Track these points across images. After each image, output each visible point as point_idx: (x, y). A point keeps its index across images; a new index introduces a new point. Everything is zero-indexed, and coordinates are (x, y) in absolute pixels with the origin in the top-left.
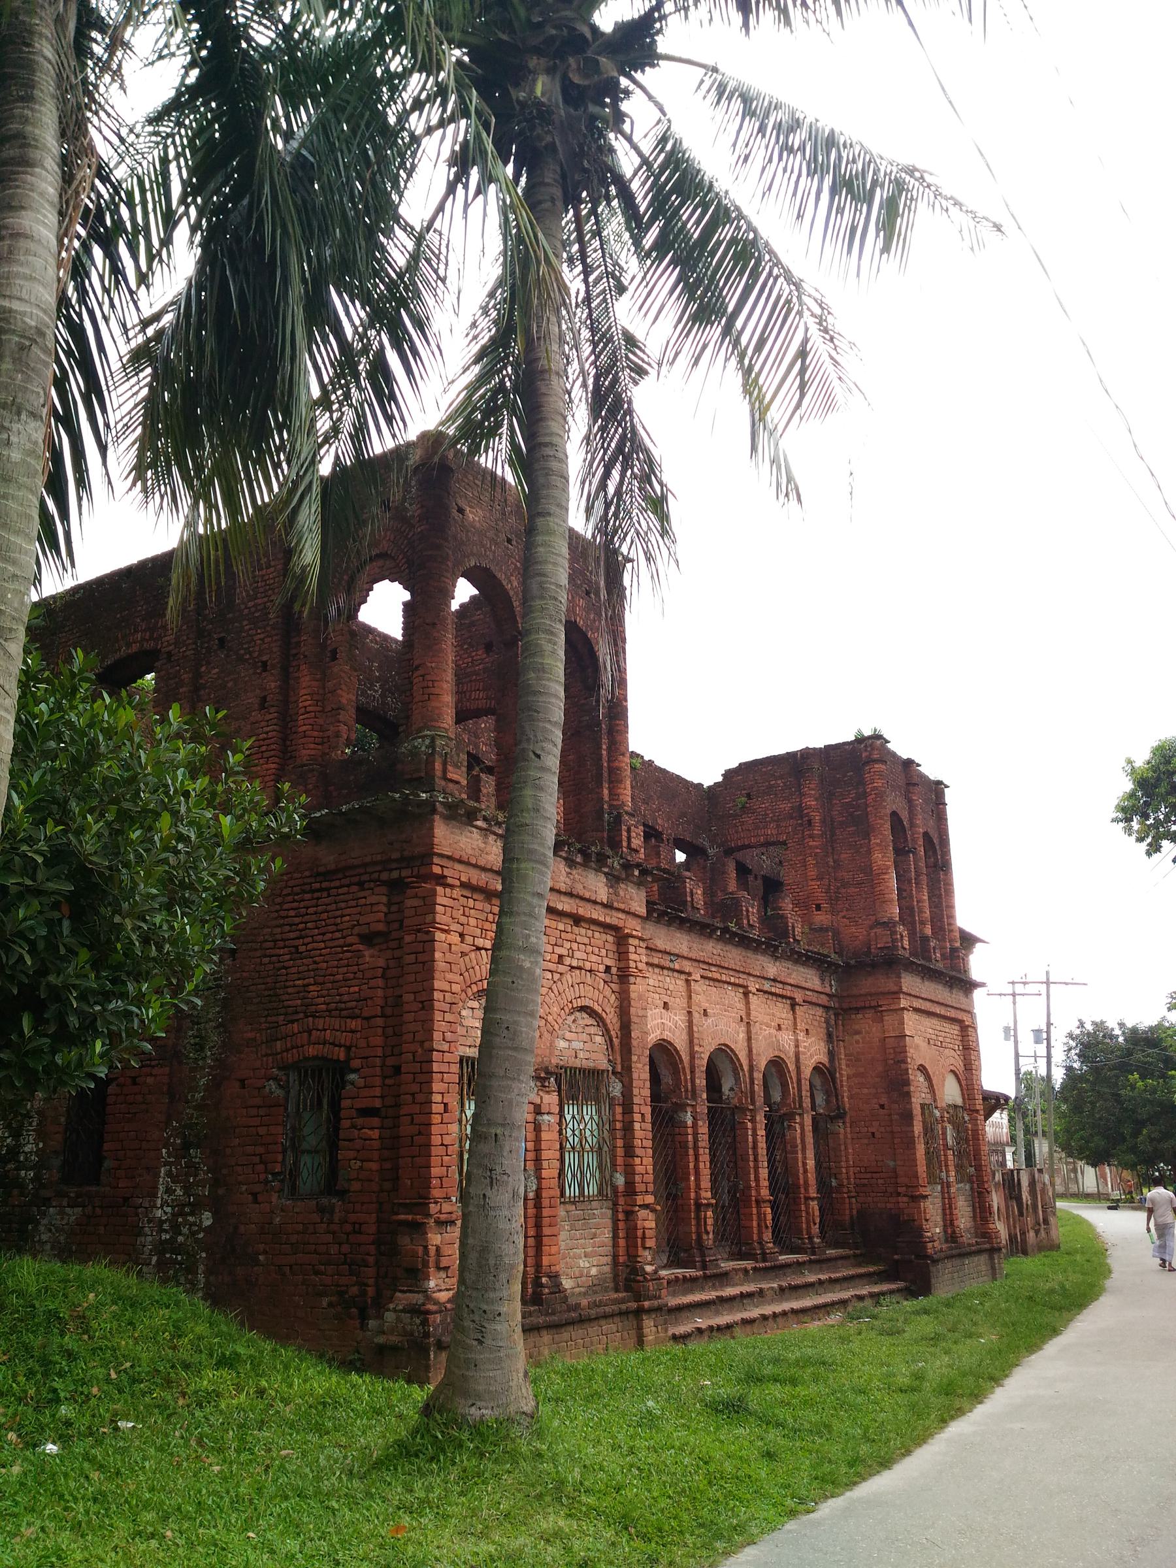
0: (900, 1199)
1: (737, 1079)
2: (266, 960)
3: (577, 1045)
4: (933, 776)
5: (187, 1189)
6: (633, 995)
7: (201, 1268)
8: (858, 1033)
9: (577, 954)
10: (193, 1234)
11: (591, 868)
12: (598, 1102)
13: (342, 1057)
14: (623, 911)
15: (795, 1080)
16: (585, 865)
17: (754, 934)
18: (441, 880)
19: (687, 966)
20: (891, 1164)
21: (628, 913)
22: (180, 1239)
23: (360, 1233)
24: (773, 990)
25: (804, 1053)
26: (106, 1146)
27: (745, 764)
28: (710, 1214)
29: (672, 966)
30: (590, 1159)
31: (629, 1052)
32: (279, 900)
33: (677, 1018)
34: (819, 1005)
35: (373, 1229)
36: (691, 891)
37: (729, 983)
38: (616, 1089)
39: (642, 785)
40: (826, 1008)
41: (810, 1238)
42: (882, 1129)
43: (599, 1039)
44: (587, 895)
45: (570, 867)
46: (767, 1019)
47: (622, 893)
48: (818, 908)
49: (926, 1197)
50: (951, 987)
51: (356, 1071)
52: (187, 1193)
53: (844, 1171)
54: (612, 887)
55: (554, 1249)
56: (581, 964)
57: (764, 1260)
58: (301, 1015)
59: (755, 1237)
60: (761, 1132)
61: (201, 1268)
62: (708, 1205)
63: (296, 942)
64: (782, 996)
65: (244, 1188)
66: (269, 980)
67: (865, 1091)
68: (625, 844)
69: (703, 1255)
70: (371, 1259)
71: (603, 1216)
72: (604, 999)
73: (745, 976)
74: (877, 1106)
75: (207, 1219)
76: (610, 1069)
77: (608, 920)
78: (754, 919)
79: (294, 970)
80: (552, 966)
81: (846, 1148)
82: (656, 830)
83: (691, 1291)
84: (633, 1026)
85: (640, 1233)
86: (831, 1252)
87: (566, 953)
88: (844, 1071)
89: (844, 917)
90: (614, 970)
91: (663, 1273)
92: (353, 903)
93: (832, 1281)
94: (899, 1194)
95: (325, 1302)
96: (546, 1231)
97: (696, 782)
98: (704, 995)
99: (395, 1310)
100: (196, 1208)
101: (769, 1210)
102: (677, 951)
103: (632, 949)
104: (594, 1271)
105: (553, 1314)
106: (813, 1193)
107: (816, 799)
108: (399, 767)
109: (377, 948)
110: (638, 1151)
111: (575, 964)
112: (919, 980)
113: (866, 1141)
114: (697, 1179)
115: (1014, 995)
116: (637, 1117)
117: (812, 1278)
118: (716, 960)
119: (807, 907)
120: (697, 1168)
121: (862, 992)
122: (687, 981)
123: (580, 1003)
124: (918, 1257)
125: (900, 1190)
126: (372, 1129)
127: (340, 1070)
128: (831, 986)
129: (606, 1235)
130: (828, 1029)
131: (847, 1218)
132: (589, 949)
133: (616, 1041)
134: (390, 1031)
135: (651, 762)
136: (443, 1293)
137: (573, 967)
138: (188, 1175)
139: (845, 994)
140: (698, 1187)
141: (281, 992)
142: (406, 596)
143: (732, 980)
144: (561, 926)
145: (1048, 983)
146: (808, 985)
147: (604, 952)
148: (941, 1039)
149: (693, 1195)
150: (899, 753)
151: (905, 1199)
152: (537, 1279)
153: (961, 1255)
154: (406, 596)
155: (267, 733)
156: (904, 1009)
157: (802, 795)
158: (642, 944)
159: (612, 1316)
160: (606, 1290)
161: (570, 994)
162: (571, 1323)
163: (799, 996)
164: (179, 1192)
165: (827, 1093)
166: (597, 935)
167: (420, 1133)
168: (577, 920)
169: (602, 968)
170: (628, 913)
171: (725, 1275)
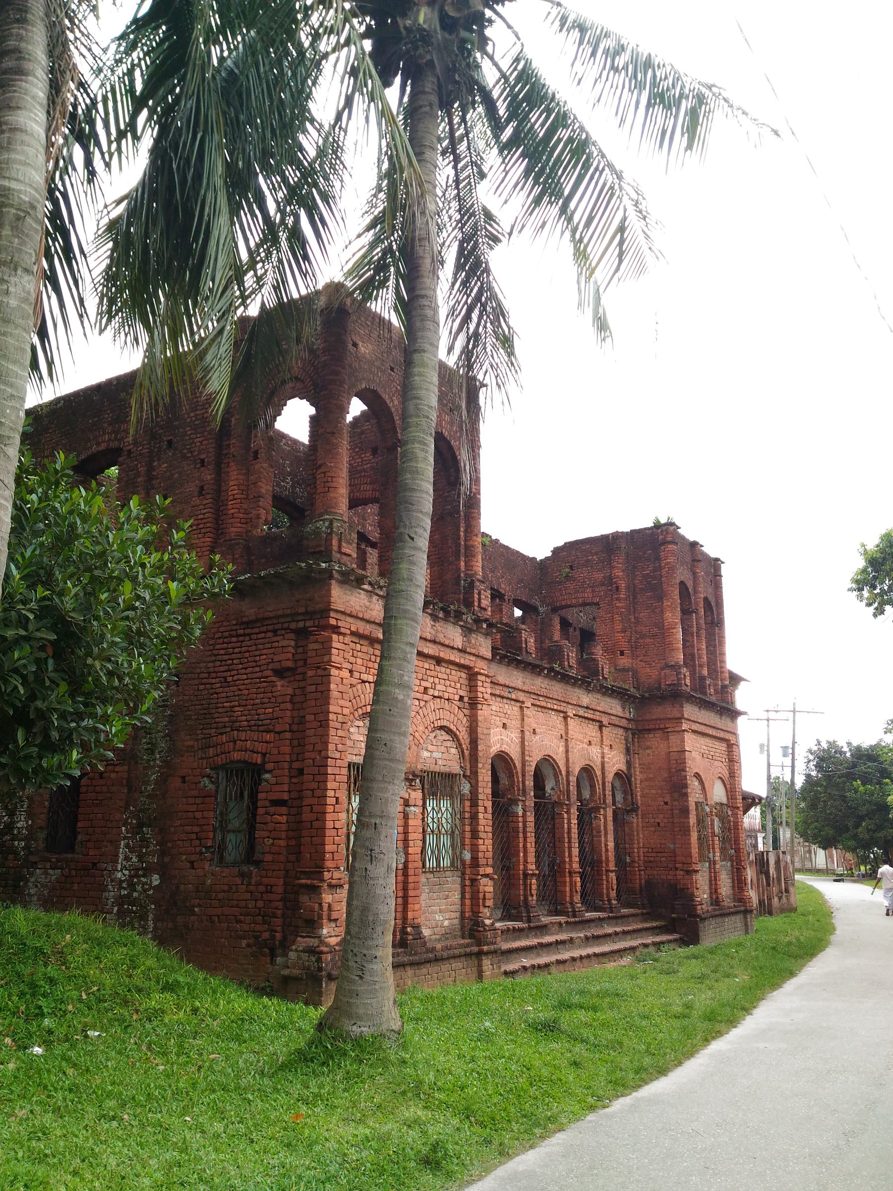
0: (678, 873)
1: (557, 781)
2: (202, 687)
3: (436, 755)
4: (713, 555)
5: (141, 857)
6: (480, 718)
7: (151, 917)
8: (649, 748)
9: (439, 687)
10: (145, 891)
11: (449, 621)
12: (452, 797)
13: (259, 761)
14: (474, 655)
15: (600, 782)
16: (446, 619)
17: (573, 673)
18: (336, 629)
19: (521, 696)
20: (672, 846)
21: (478, 656)
22: (135, 894)
23: (271, 892)
24: (586, 715)
25: (608, 763)
26: (79, 824)
27: (569, 543)
28: (534, 881)
29: (510, 696)
30: (446, 840)
31: (476, 761)
32: (211, 642)
33: (513, 735)
34: (621, 727)
35: (280, 890)
36: (526, 639)
37: (553, 710)
38: (466, 788)
39: (490, 558)
40: (626, 729)
41: (609, 900)
42: (666, 821)
43: (453, 751)
44: (447, 642)
45: (434, 621)
46: (580, 737)
47: (473, 641)
48: (622, 653)
49: (697, 871)
50: (721, 715)
51: (269, 772)
52: (141, 860)
53: (636, 850)
55: (417, 907)
56: (441, 694)
57: (574, 916)
58: (229, 729)
59: (568, 899)
60: (574, 821)
61: (151, 917)
62: (533, 875)
63: (225, 674)
64: (593, 720)
65: (184, 857)
66: (204, 702)
67: (653, 791)
68: (476, 604)
69: (528, 912)
70: (279, 912)
71: (453, 883)
72: (458, 721)
73: (565, 705)
74: (662, 803)
75: (156, 880)
76: (462, 773)
77: (462, 662)
78: (573, 662)
79: (224, 695)
80: (419, 696)
81: (638, 834)
82: (500, 592)
83: (518, 938)
84: (480, 742)
85: (481, 895)
86: (625, 911)
87: (429, 685)
88: (638, 776)
89: (641, 661)
90: (466, 699)
91: (498, 925)
92: (269, 646)
93: (624, 933)
94: (677, 869)
95: (244, 943)
96: (411, 893)
97: (531, 556)
98: (534, 718)
99: (296, 950)
100: (148, 871)
101: (579, 879)
102: (514, 685)
103: (480, 683)
104: (446, 923)
105: (415, 954)
106: (612, 866)
107: (623, 571)
108: (305, 542)
109: (287, 680)
110: (482, 835)
111: (436, 694)
112: (697, 709)
113: (653, 829)
114: (525, 856)
115: (768, 720)
116: (481, 809)
117: (610, 930)
118: (544, 692)
119: (614, 653)
120: (525, 847)
121: (654, 717)
122: (521, 707)
123: (439, 723)
124: (690, 916)
125: (678, 866)
126: (282, 815)
127: (257, 771)
128: (630, 712)
129: (456, 897)
130: (626, 745)
131: (637, 886)
132: (448, 683)
133: (467, 753)
134: (295, 742)
135: (497, 541)
136: (333, 939)
137: (435, 697)
138: (141, 847)
139: (640, 719)
140: (526, 861)
141: (213, 711)
142: (312, 411)
143: (555, 707)
144: (427, 666)
145: (794, 711)
146: (613, 712)
147: (458, 685)
148: (712, 753)
149: (521, 867)
150: (687, 537)
151: (682, 873)
152: (404, 928)
153: (723, 915)
154: (312, 411)
155: (204, 514)
156: (684, 731)
157: (612, 568)
158: (488, 680)
159: (460, 956)
160: (455, 937)
161: (432, 717)
162: (429, 961)
163: (605, 721)
164: (134, 859)
165: (625, 792)
166: (453, 672)
167: (317, 819)
168: (439, 661)
169: (457, 697)
170: (478, 656)
171: (545, 926)
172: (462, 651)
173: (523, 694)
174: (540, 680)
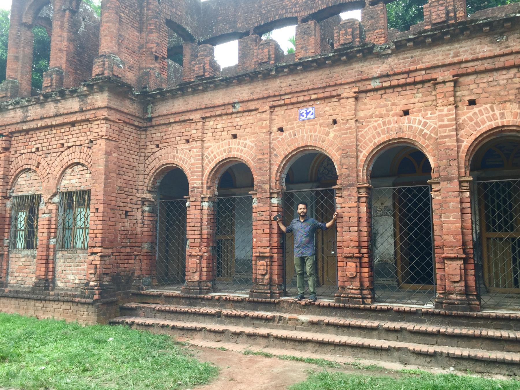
3: (72, 181)
19: (252, 106)
24: (384, 85)
29: (234, 110)
43: (88, 176)
47: (89, 101)
54: (82, 101)
56: (73, 144)
64: (415, 83)
102: (236, 100)
104: (77, 281)
111: (70, 144)
123: (71, 162)
137: (69, 147)
143: (314, 97)
158: (102, 122)
161: (66, 159)
163: (440, 75)
168: (73, 124)
170: (94, 109)
172: (81, 111)
173: (256, 102)
174: (278, 81)
